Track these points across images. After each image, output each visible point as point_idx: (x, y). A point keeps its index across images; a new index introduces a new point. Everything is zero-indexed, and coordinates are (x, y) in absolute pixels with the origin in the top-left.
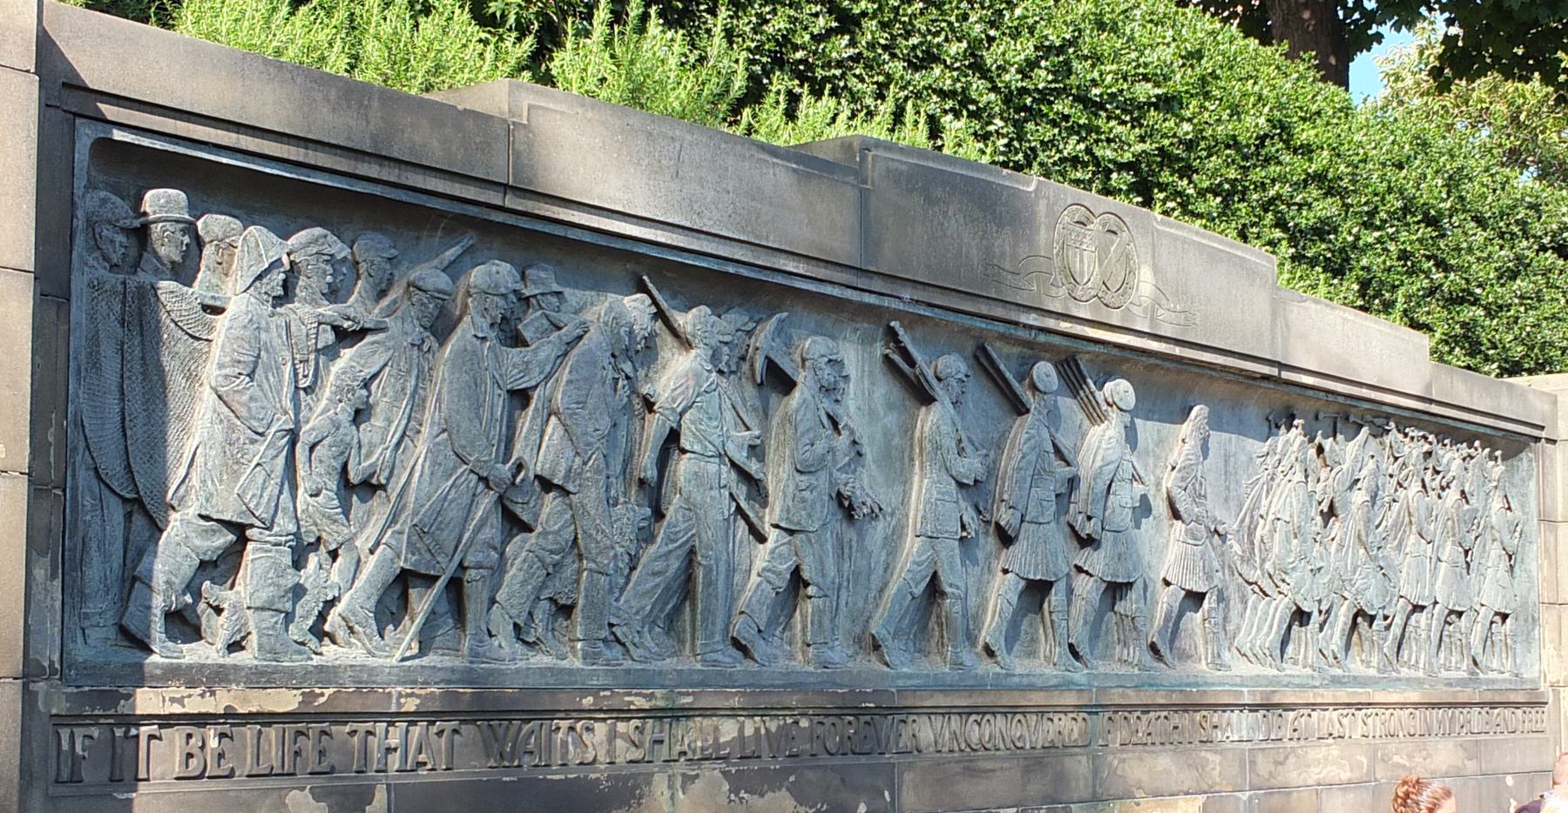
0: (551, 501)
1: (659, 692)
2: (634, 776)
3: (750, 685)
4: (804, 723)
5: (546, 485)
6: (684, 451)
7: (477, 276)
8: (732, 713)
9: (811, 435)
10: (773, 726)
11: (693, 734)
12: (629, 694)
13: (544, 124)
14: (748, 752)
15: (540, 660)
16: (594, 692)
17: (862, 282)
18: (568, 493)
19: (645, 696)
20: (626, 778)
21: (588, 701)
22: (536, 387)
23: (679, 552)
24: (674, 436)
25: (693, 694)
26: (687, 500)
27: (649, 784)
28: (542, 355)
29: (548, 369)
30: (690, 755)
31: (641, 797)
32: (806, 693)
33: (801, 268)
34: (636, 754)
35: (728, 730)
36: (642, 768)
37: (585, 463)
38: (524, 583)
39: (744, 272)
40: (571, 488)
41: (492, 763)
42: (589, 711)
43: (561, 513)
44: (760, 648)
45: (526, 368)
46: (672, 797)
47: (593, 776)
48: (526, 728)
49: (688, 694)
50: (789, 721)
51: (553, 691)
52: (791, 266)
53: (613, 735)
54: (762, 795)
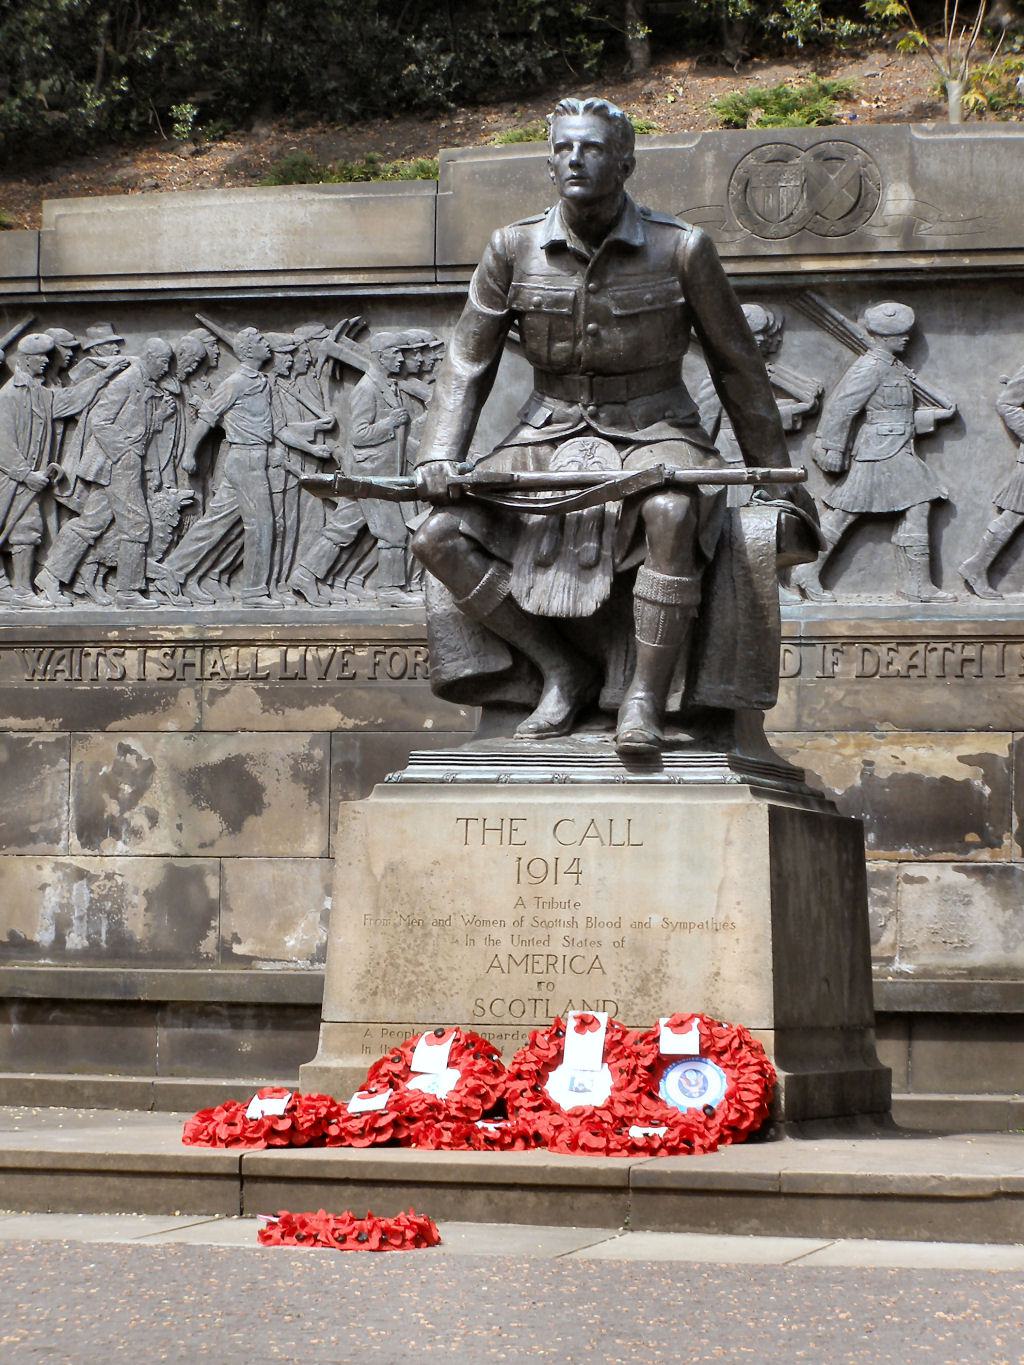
0: (94, 494)
1: (185, 627)
2: (160, 690)
3: (298, 622)
4: (361, 653)
5: (88, 484)
6: (231, 443)
7: (24, 343)
8: (272, 644)
9: (370, 415)
10: (324, 654)
11: (230, 660)
12: (156, 629)
13: (69, 226)
14: (289, 674)
15: (81, 606)
16: (121, 629)
17: (442, 276)
18: (103, 486)
19: (171, 631)
20: (152, 691)
21: (114, 634)
22: (81, 411)
23: (224, 521)
24: (215, 436)
25: (222, 628)
26: (230, 482)
27: (176, 696)
28: (85, 390)
29: (89, 399)
30: (223, 675)
31: (168, 704)
32: (357, 627)
33: (361, 278)
34: (168, 673)
35: (269, 657)
36: (170, 683)
37: (115, 463)
38: (68, 552)
39: (292, 294)
40: (103, 482)
41: (27, 677)
42: (115, 641)
43: (99, 502)
44: (311, 592)
45: (71, 402)
46: (200, 706)
47: (118, 688)
48: (58, 653)
49: (217, 629)
50: (339, 650)
51: (78, 628)
52: (347, 279)
53: (144, 660)
54: (302, 707)
